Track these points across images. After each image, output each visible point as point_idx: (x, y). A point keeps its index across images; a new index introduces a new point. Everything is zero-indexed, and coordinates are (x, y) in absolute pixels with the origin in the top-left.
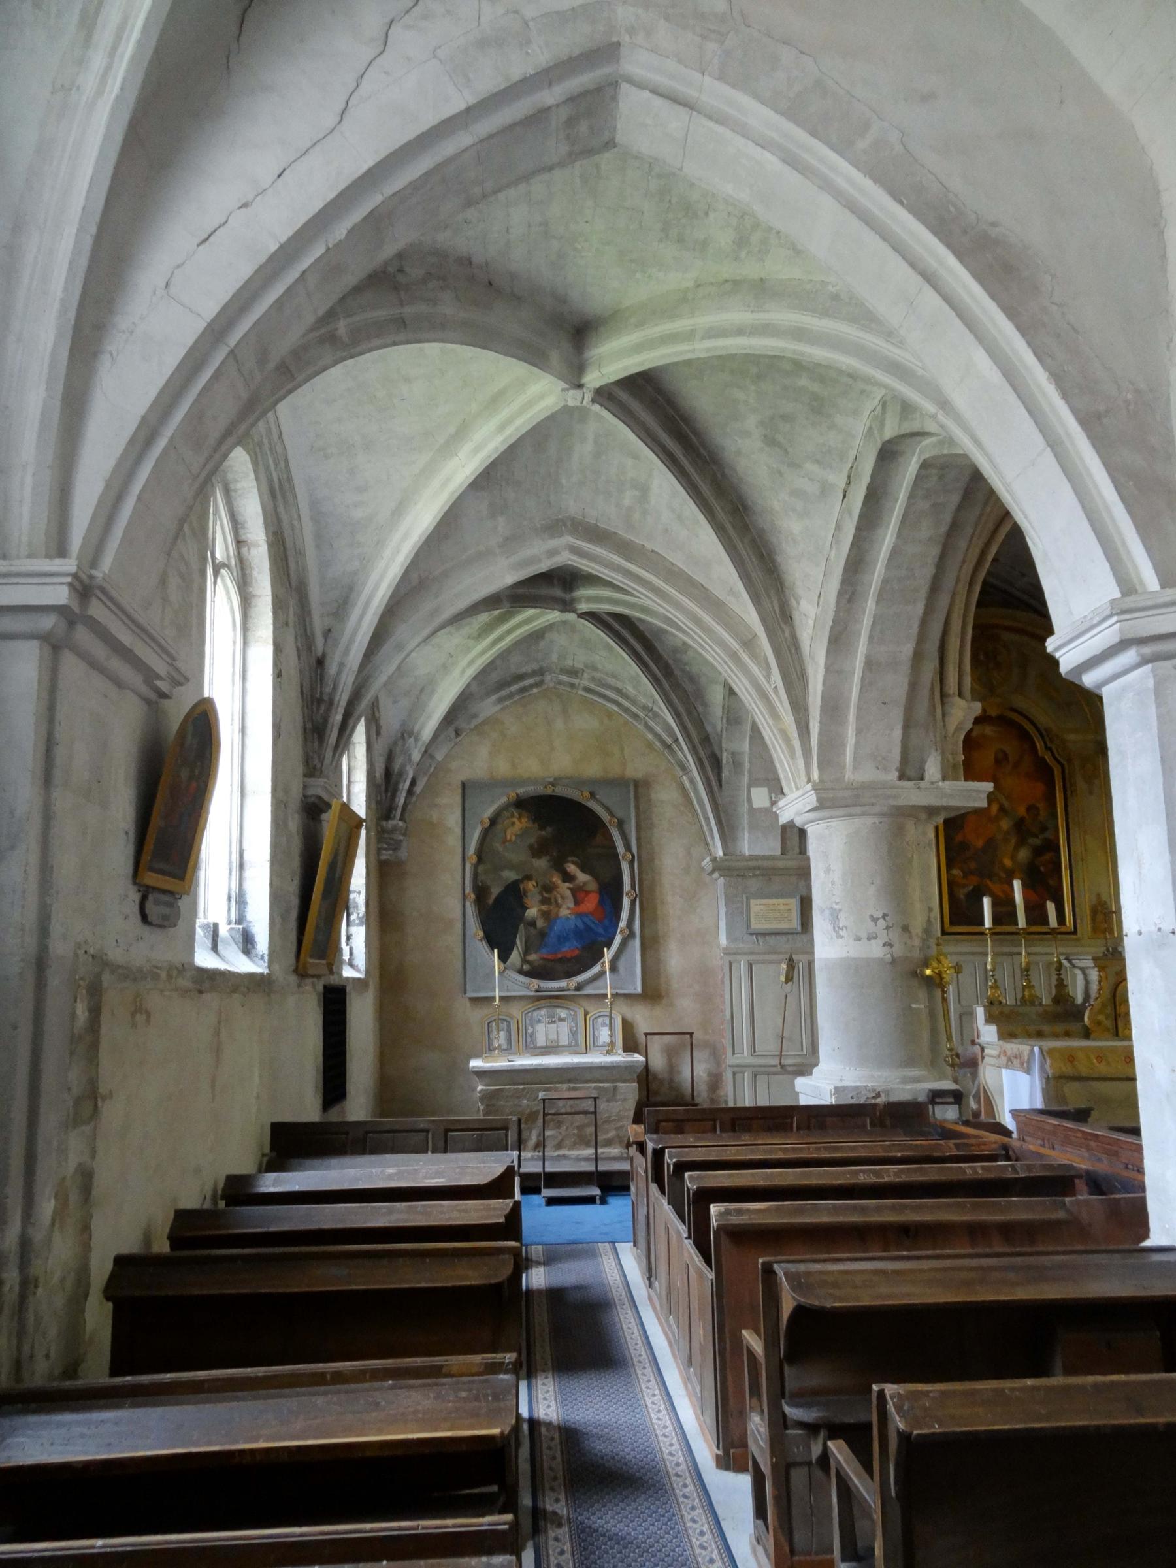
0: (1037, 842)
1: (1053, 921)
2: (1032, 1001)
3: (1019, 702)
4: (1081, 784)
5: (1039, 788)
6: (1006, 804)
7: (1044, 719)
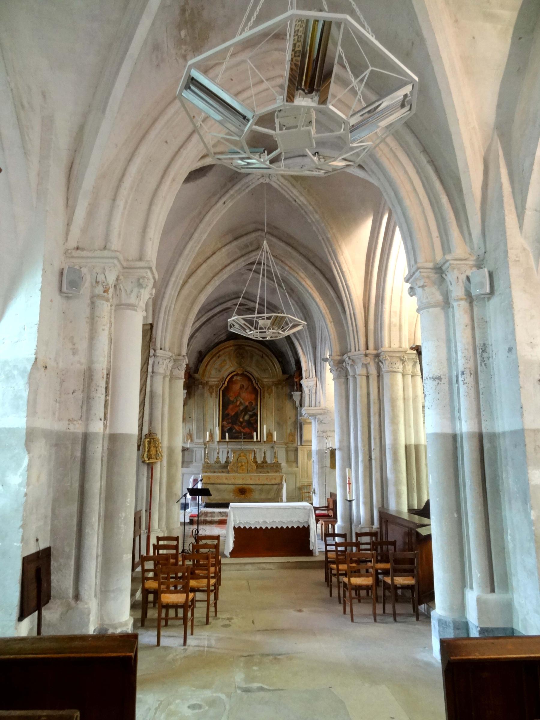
0: (251, 413)
1: (255, 439)
2: (217, 462)
3: (249, 369)
4: (267, 395)
5: (254, 396)
6: (242, 401)
7: (256, 375)
